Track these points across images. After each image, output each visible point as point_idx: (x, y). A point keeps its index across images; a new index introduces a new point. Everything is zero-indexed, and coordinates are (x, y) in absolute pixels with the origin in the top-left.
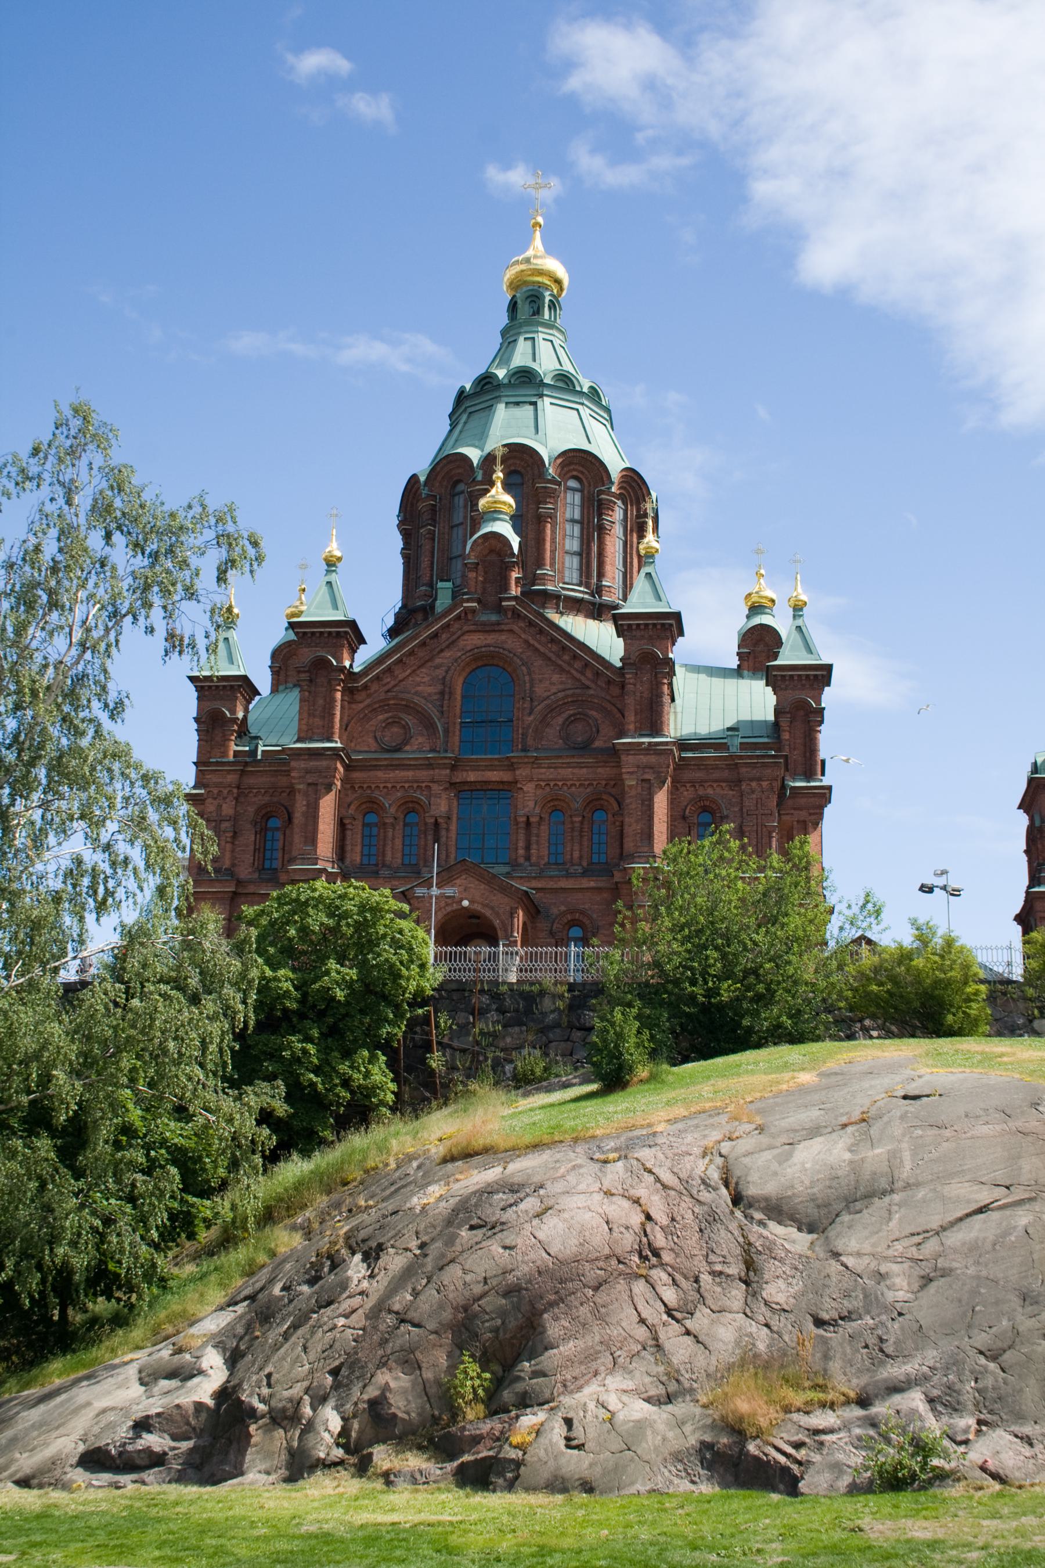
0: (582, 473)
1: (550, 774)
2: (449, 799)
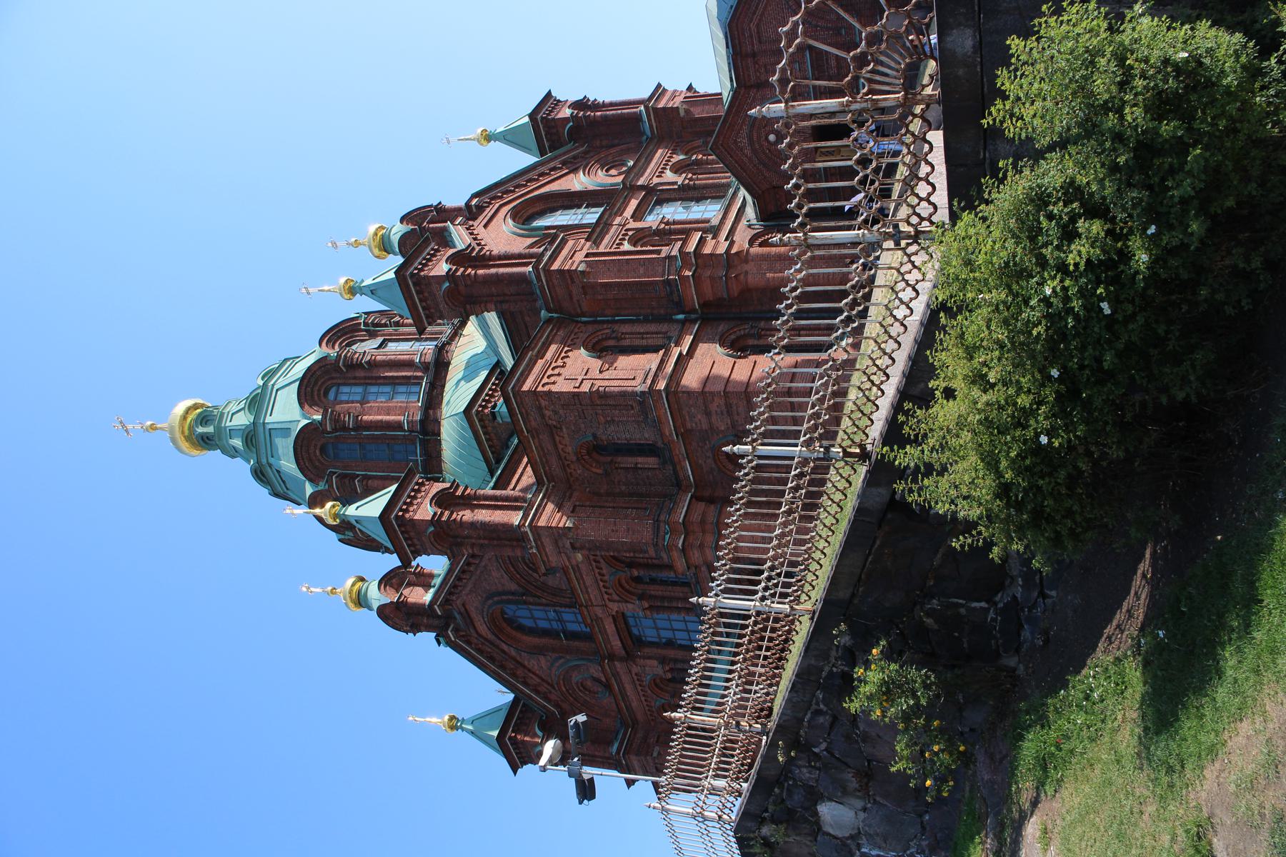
0: (316, 445)
1: (594, 593)
2: (644, 658)
